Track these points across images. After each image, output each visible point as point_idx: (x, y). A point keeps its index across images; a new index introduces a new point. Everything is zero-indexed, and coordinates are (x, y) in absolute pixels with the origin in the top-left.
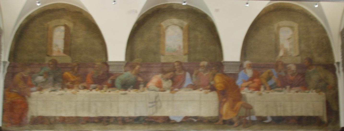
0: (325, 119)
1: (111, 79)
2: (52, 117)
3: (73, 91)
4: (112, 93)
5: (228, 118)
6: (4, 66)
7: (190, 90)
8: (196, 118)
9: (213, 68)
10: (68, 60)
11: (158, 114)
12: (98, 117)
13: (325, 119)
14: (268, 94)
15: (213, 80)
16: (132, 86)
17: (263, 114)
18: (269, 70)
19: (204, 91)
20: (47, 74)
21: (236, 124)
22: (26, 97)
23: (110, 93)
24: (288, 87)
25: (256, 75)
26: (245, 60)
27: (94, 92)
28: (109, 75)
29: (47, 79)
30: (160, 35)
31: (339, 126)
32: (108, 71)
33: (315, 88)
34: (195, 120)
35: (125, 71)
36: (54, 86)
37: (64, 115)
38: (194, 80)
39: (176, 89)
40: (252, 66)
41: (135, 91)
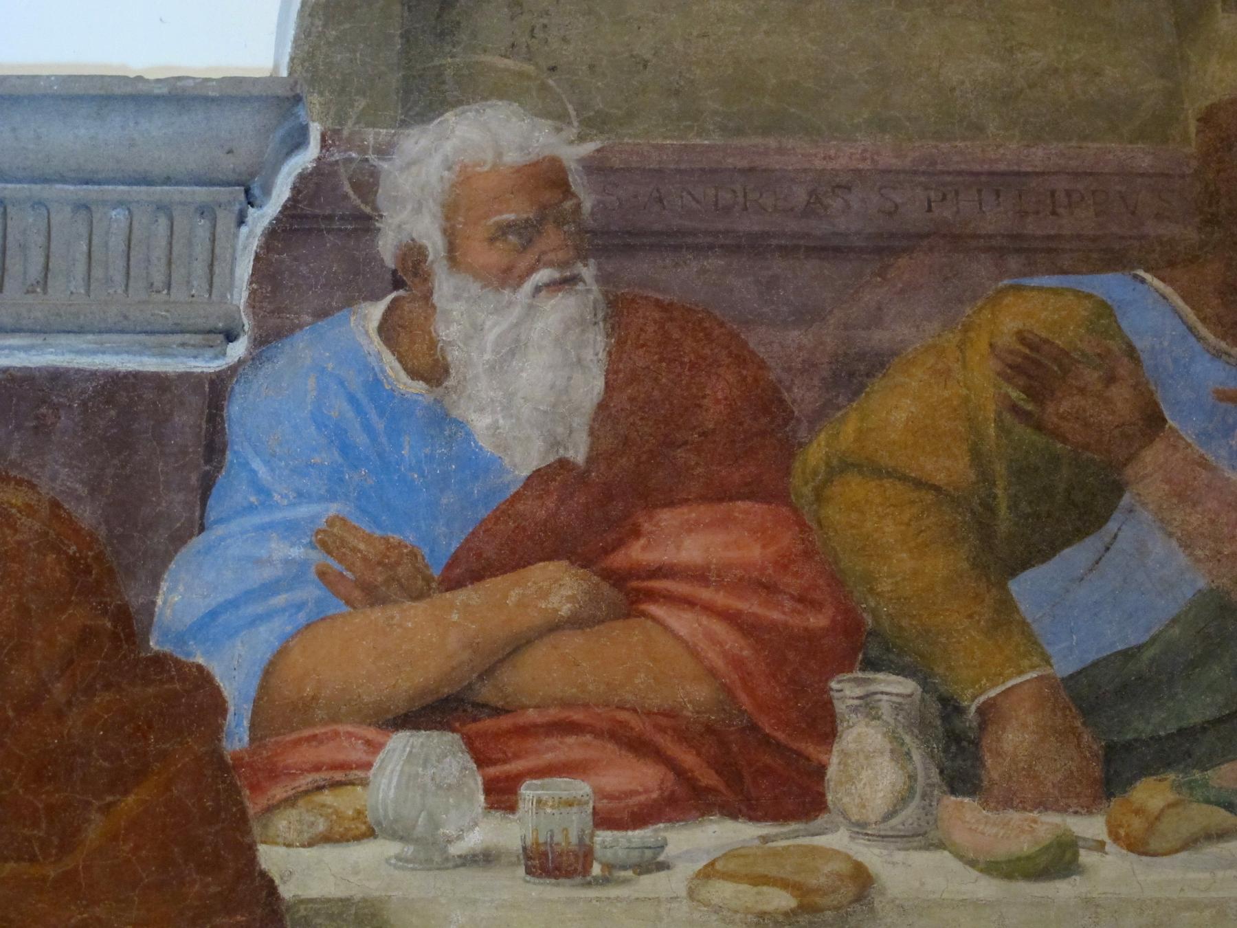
14: (1063, 889)
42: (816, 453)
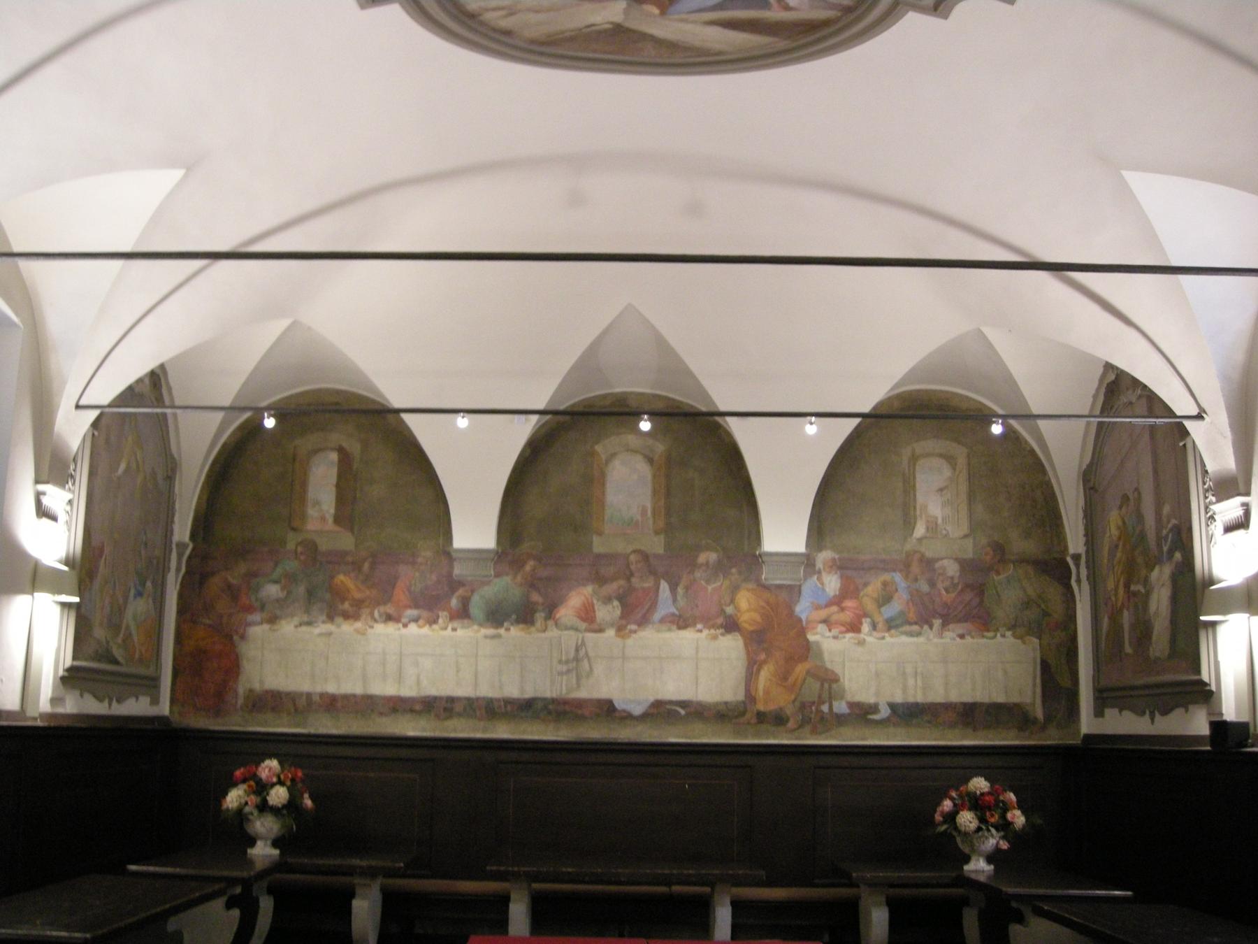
0: (1039, 713)
2: (301, 694)
3: (358, 625)
4: (460, 632)
5: (772, 707)
6: (180, 556)
7: (670, 630)
8: (684, 704)
9: (734, 570)
10: (346, 541)
11: (583, 694)
12: (425, 697)
13: (1039, 713)
14: (884, 641)
15: (732, 601)
16: (514, 617)
17: (868, 698)
18: (886, 577)
19: (706, 632)
20: (289, 580)
21: (791, 724)
22: (235, 638)
23: (454, 633)
24: (937, 623)
25: (849, 591)
26: (820, 549)
27: (413, 628)
28: (454, 585)
29: (289, 593)
30: (593, 480)
31: (1078, 731)
32: (450, 574)
33: (1012, 627)
34: (683, 712)
35: (498, 575)
36: (307, 611)
37: (331, 688)
38: (682, 602)
39: (633, 627)
40: (840, 566)
41: (523, 630)
42: (862, 594)
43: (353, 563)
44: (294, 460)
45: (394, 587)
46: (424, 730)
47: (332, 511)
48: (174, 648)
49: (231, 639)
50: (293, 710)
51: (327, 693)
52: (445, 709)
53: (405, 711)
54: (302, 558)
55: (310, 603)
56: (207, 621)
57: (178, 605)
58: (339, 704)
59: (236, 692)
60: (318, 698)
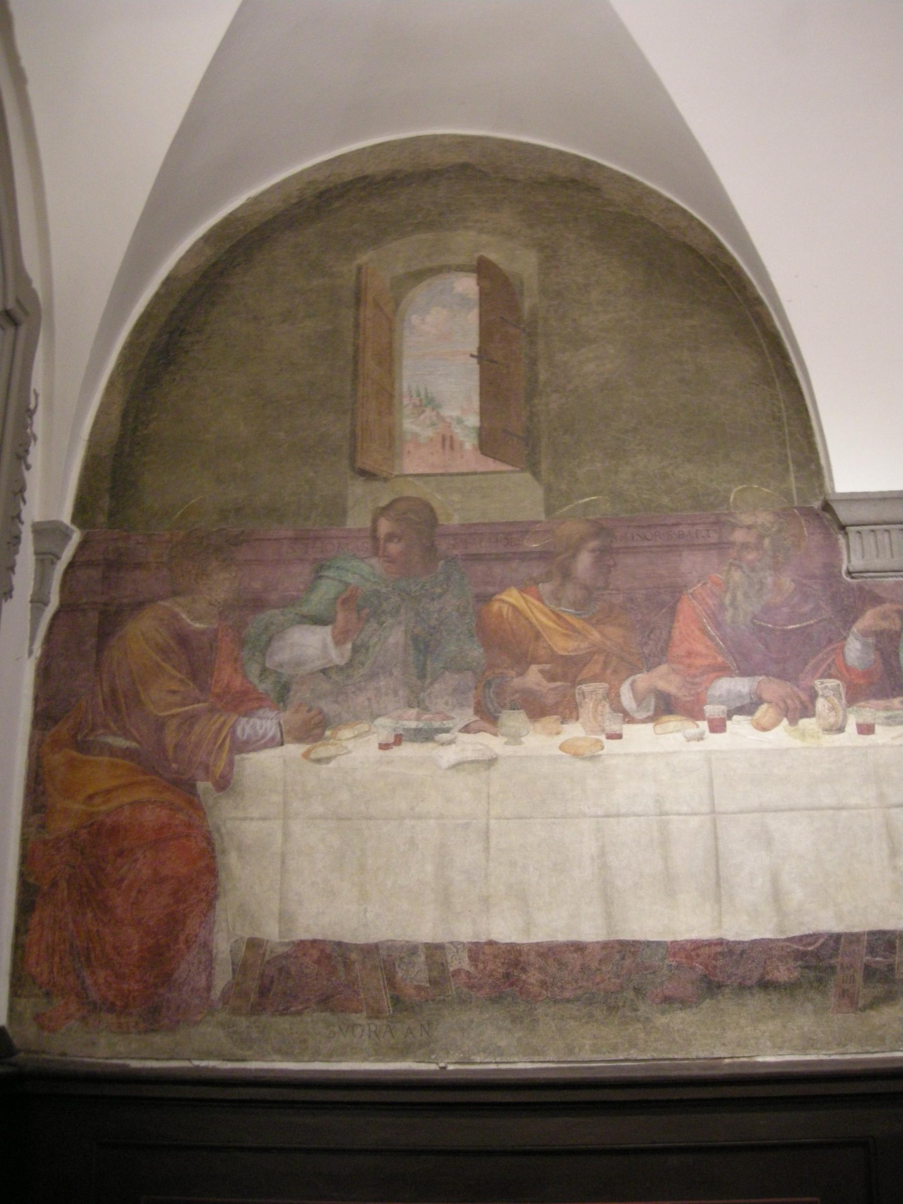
1: (865, 634)
2: (413, 949)
3: (574, 731)
4: (883, 735)
6: (45, 559)
22: (203, 786)
27: (739, 726)
32: (831, 573)
36: (416, 701)
43: (543, 556)
44: (358, 300)
45: (673, 612)
46: (809, 1044)
47: (473, 421)
48: (25, 825)
49: (191, 788)
50: (386, 1003)
51: (491, 943)
52: (870, 973)
53: (743, 988)
54: (394, 548)
55: (422, 676)
56: (121, 742)
57: (36, 699)
58: (533, 977)
59: (206, 946)
60: (466, 965)
